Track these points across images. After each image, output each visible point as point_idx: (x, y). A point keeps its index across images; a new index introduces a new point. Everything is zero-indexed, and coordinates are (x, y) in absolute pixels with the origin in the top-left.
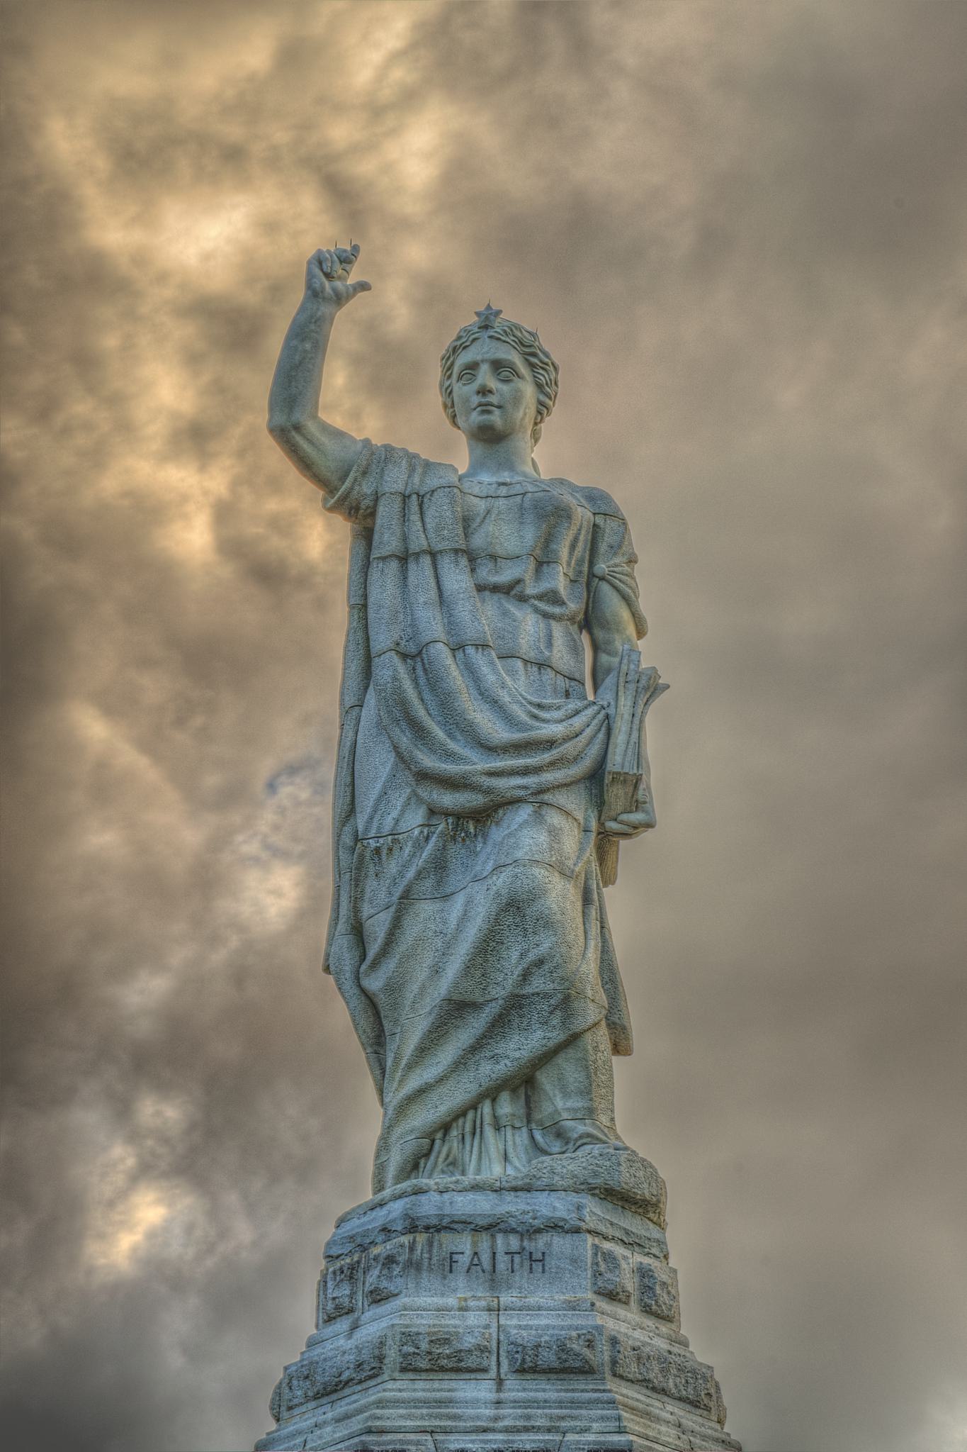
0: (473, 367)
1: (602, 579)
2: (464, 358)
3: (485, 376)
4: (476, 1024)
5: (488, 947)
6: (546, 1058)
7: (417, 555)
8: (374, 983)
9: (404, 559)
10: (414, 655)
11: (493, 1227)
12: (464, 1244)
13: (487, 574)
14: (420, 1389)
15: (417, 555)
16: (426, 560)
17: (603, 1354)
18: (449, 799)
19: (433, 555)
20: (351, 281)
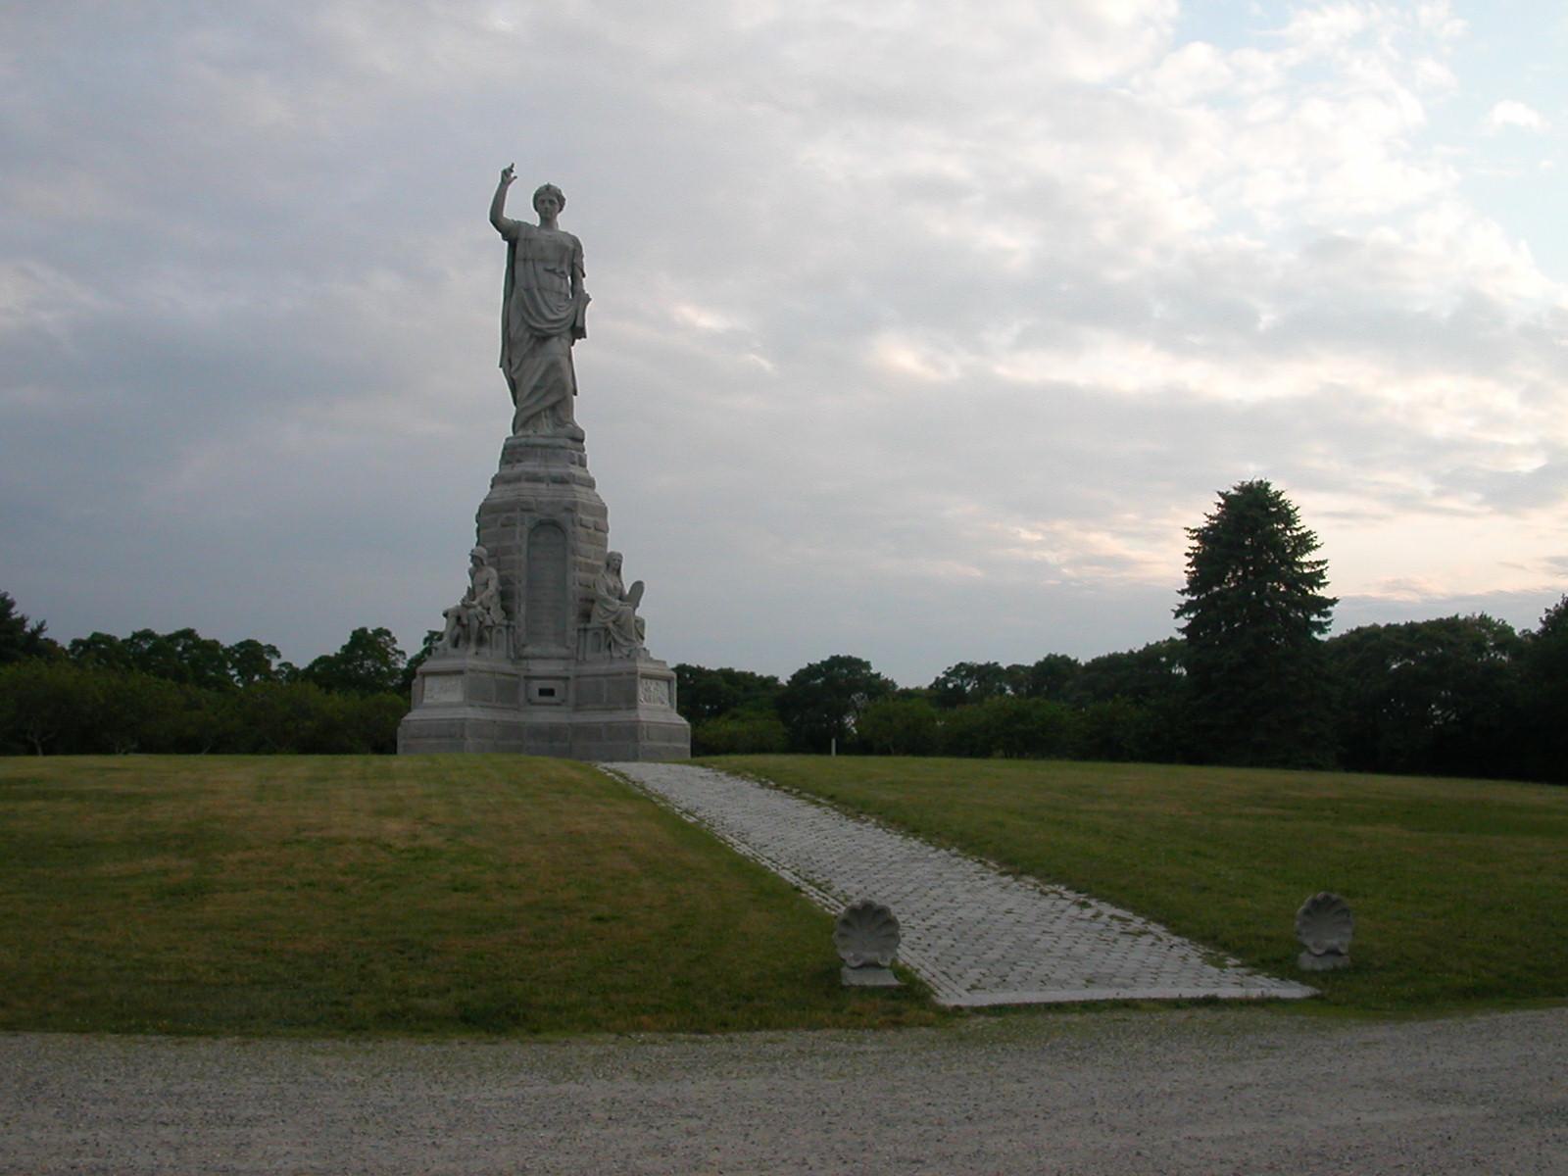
0: (543, 201)
2: (540, 198)
3: (548, 205)
4: (540, 393)
6: (559, 402)
8: (515, 377)
9: (525, 260)
10: (528, 290)
11: (546, 446)
12: (539, 450)
14: (530, 485)
18: (536, 333)
19: (533, 260)
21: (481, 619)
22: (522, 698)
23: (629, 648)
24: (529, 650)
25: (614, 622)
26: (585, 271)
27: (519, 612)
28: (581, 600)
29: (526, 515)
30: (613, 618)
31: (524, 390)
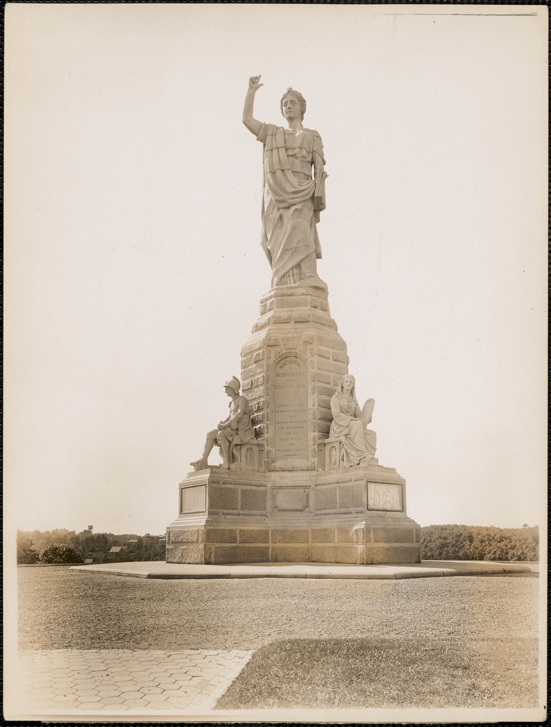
1: (315, 151)
5: (290, 238)
7: (274, 149)
13: (290, 152)
15: (274, 149)
16: (276, 150)
17: (311, 318)
20: (259, 83)
21: (230, 439)
22: (269, 504)
23: (359, 458)
24: (278, 464)
25: (346, 435)
26: (325, 158)
27: (268, 433)
28: (320, 419)
29: (273, 350)
30: (345, 432)
31: (277, 255)
